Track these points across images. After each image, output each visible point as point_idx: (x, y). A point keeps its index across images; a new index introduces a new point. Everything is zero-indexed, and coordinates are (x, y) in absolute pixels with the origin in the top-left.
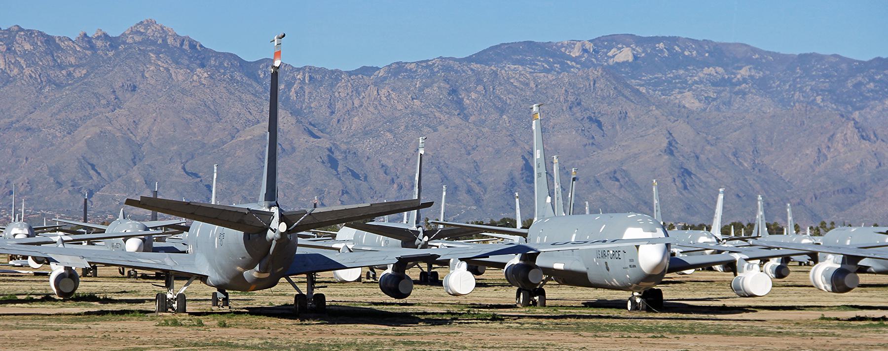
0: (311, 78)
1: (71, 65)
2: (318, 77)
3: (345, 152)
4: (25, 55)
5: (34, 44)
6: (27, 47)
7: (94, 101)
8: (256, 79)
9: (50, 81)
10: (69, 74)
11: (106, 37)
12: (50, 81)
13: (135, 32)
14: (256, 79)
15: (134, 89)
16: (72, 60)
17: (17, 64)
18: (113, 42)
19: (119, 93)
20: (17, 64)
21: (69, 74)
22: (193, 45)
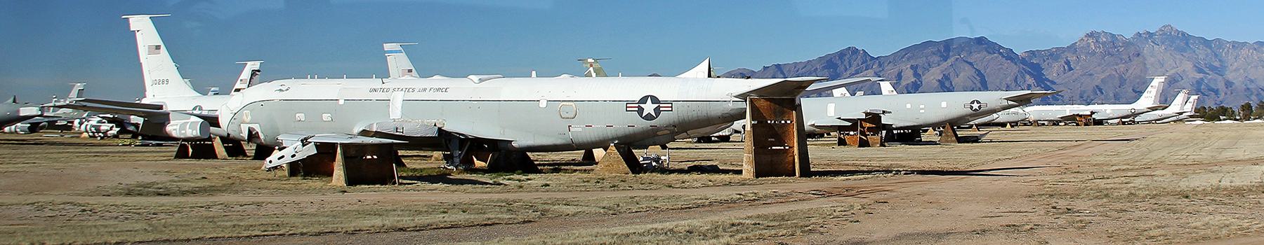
0: (1233, 46)
1: (1120, 46)
2: (1236, 45)
3: (1209, 79)
4: (1104, 43)
5: (1107, 39)
6: (1104, 40)
7: (1119, 62)
8: (1211, 48)
9: (1109, 54)
10: (1118, 50)
11: (1148, 33)
12: (1109, 54)
13: (1161, 30)
14: (1211, 48)
15: (1138, 55)
16: (1121, 44)
17: (1099, 47)
18: (1150, 35)
19: (1131, 58)
20: (1099, 47)
21: (1118, 50)
22: (1183, 34)
